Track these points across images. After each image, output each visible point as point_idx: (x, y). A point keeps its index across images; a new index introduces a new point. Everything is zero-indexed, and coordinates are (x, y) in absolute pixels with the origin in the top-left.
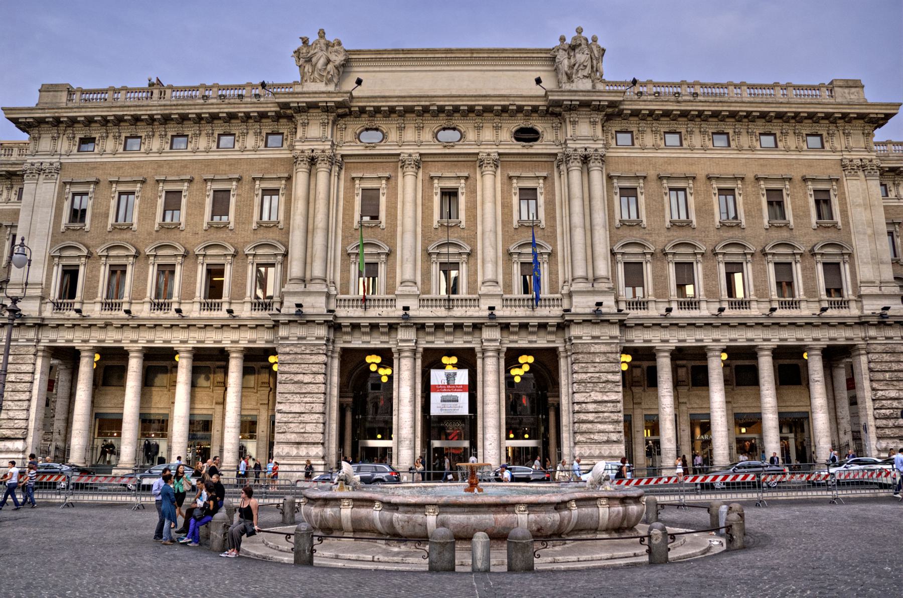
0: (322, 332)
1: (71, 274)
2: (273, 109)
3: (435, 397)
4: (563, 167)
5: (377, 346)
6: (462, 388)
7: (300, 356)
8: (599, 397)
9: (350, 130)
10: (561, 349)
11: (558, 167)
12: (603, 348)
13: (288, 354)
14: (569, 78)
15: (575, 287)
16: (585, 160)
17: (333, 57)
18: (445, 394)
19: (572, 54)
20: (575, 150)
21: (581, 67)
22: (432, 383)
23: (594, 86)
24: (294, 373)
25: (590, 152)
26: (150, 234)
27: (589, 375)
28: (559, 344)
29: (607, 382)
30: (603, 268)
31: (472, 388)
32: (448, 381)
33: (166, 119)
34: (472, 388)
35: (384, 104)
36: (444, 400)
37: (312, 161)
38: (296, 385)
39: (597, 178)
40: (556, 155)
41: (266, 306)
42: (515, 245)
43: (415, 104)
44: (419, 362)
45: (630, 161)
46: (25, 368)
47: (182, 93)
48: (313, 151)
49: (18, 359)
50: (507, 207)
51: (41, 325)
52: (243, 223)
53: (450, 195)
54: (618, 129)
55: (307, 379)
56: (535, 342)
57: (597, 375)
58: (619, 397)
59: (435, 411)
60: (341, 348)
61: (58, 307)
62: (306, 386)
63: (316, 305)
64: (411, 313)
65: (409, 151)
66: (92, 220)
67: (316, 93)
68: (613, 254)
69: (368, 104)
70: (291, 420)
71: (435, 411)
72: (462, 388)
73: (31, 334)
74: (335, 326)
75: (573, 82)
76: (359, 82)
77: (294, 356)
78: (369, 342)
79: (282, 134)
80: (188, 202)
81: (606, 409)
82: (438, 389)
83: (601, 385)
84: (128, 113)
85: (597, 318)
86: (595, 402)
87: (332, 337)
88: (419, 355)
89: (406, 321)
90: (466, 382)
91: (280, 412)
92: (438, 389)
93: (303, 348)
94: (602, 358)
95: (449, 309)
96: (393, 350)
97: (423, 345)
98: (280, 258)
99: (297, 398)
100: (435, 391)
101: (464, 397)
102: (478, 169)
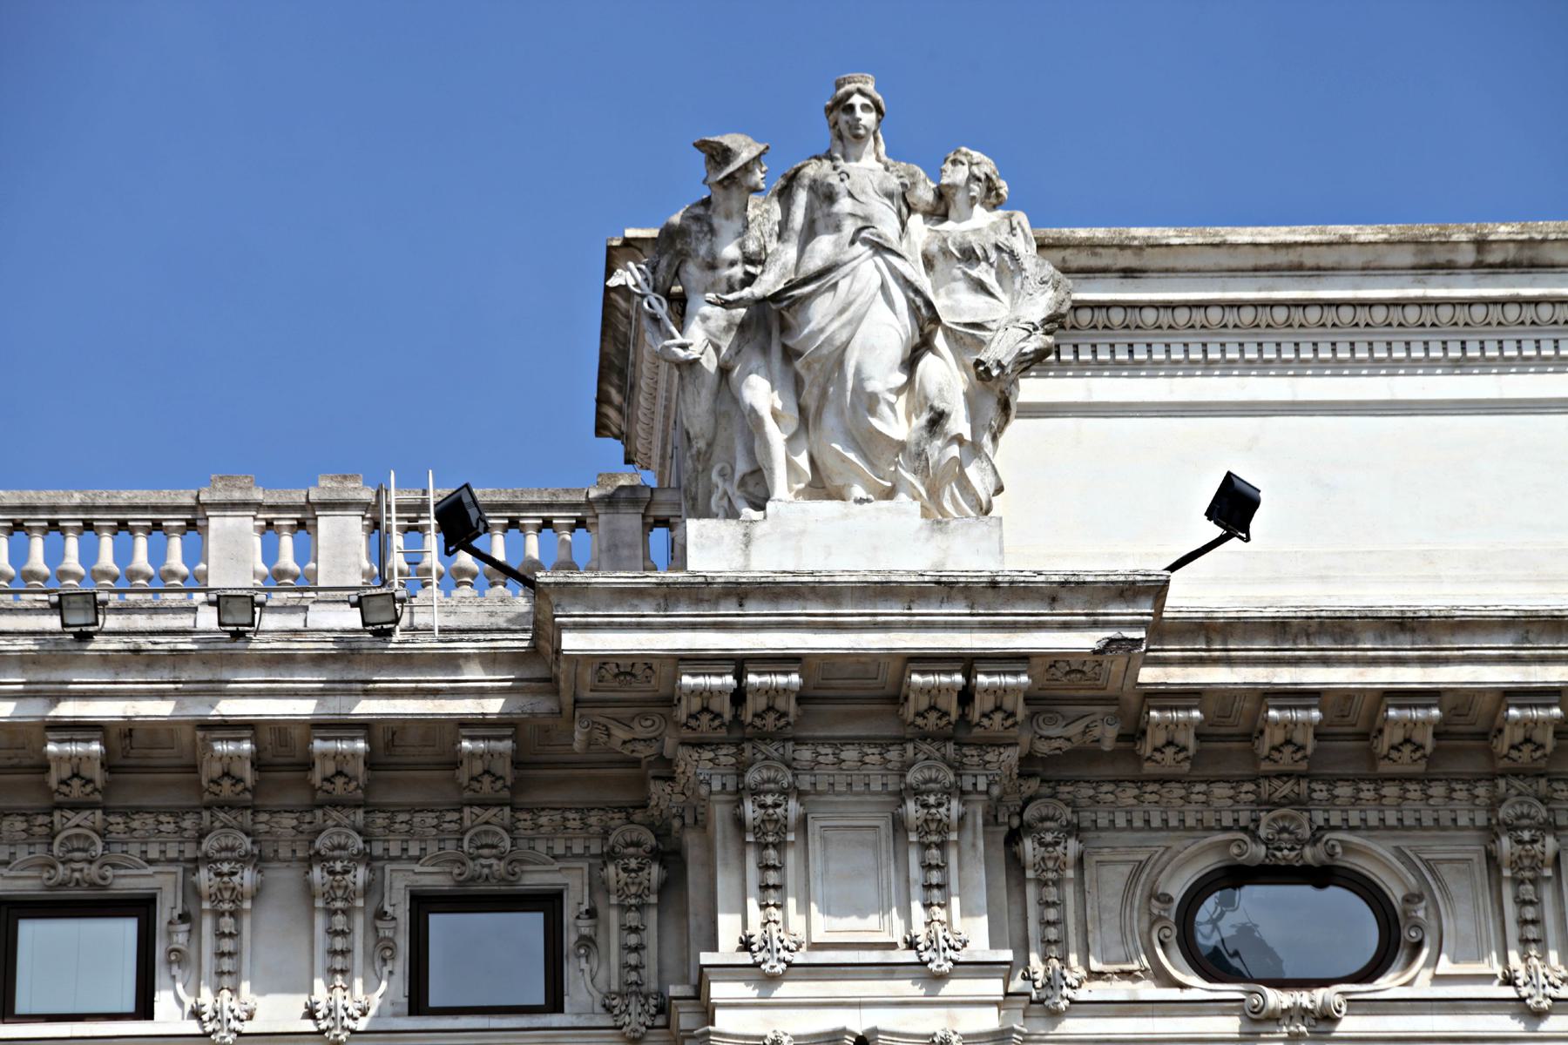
2: (494, 706)
9: (1111, 880)
17: (956, 304)
67: (884, 590)
69: (1284, 676)
76: (1234, 507)
79: (549, 903)
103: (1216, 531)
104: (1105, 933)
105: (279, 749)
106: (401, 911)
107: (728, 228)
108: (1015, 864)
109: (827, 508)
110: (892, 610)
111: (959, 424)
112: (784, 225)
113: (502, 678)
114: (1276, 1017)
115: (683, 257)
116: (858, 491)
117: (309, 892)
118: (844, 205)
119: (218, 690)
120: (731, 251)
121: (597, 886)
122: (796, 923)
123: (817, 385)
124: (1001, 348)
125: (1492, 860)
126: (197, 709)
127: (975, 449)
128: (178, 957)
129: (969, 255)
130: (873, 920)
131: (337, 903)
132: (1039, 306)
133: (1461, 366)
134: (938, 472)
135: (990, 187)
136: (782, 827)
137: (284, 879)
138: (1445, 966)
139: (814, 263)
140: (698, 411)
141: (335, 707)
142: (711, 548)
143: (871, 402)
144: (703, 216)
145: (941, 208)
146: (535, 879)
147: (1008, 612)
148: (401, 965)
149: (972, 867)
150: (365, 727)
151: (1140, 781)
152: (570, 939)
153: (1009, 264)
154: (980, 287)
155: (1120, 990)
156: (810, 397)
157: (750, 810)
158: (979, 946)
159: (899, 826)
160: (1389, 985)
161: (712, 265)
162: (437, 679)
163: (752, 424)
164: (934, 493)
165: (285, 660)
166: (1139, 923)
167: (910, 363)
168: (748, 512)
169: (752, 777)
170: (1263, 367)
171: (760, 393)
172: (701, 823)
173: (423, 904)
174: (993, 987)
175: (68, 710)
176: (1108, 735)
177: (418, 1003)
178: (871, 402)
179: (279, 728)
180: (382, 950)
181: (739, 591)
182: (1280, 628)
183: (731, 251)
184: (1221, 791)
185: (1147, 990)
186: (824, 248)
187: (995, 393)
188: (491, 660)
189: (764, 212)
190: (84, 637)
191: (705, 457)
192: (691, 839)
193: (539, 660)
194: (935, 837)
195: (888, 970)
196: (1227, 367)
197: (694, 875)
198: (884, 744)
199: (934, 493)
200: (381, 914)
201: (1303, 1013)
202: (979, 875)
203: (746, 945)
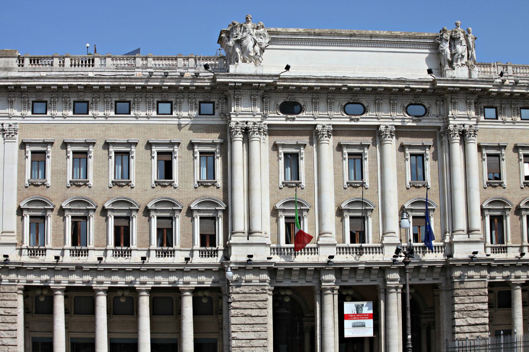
0: (265, 276)
1: (38, 222)
2: (209, 84)
3: (347, 323)
4: (445, 138)
5: (303, 285)
6: (369, 316)
7: (248, 295)
8: (472, 321)
10: (443, 285)
11: (441, 137)
12: (475, 285)
13: (238, 293)
14: (451, 64)
15: (456, 238)
16: (463, 134)
17: (259, 40)
18: (355, 321)
19: (453, 44)
20: (455, 126)
21: (460, 56)
23: (470, 73)
24: (244, 309)
25: (467, 127)
26: (104, 190)
27: (466, 305)
28: (441, 281)
29: (479, 310)
30: (477, 223)
31: (376, 317)
33: (114, 89)
35: (305, 84)
37: (246, 132)
38: (247, 318)
39: (473, 148)
40: (439, 128)
41: (214, 253)
42: (409, 203)
43: (330, 84)
44: (336, 297)
45: (495, 132)
46: (10, 304)
47: (119, 62)
48: (247, 122)
49: (3, 296)
50: (400, 170)
51: (21, 269)
52: (186, 182)
53: (356, 158)
54: (486, 105)
55: (254, 313)
57: (471, 305)
58: (487, 321)
61: (33, 252)
62: (254, 318)
63: (261, 255)
64: (334, 260)
65: (324, 123)
66: (51, 176)
67: (251, 75)
68: (482, 210)
69: (292, 84)
70: (244, 345)
71: (349, 333)
72: (369, 316)
73: (13, 276)
74: (273, 271)
75: (454, 69)
76: (288, 68)
77: (243, 295)
80: (137, 162)
81: (477, 330)
82: (349, 317)
83: (474, 312)
84: (82, 83)
85: (473, 263)
86: (470, 325)
89: (329, 266)
90: (371, 312)
91: (234, 339)
92: (349, 317)
93: (250, 288)
94: (476, 292)
95: (361, 255)
98: (220, 214)
99: (247, 328)
100: (347, 319)
101: (370, 323)
102: (377, 138)
103: (285, 70)
104: (272, 108)
105: (186, 87)
106: (198, 103)
107: (234, 31)
108: (263, 101)
109: (245, 64)
110: (251, 77)
111: (259, 54)
112: (241, 30)
113: (210, 81)
114: (289, 118)
115: (229, 34)
116: (248, 62)
117: (188, 101)
118: (247, 29)
119: (180, 82)
120: (235, 34)
121: (219, 101)
122: (240, 108)
123: (244, 50)
124: (263, 46)
125: (312, 102)
126: (178, 84)
127: (260, 56)
128: (175, 108)
129: (260, 35)
130: (248, 108)
131: (191, 103)
132: (267, 41)
133: (312, 45)
134: (256, 59)
135: (263, 26)
136: (239, 98)
137: (186, 100)
138: (307, 113)
139: (244, 36)
140: (231, 51)
141: (192, 84)
142: (232, 69)
143: (250, 52)
144: (232, 30)
145: (257, 28)
146: (212, 100)
147: (264, 78)
148: (198, 109)
149: (259, 102)
150: (195, 86)
151: (276, 92)
152: (216, 107)
153: (264, 36)
154: (261, 38)
155: (273, 115)
156: (243, 50)
157: (236, 97)
158: (259, 112)
159: (251, 98)
160: (300, 115)
161: (233, 35)
162: (203, 81)
163: (237, 54)
164: (256, 61)
165: (187, 79)
166: (275, 107)
167: (254, 47)
168: (236, 63)
169: (236, 93)
170: (291, 45)
171: (238, 50)
172: (230, 96)
173: (200, 102)
174: (260, 116)
175: (165, 84)
176: (273, 89)
177: (200, 114)
178: (250, 52)
179: (186, 86)
180: (196, 108)
181: (236, 75)
182: (292, 79)
183: (235, 34)
184: (285, 94)
185: (276, 115)
186: (245, 34)
187: (262, 50)
188: (208, 79)
189: (238, 29)
190: (166, 76)
191: (231, 55)
192: (229, 98)
193: (214, 79)
194: (255, 100)
195: (249, 114)
196: (287, 45)
197: (229, 102)
198: (250, 90)
199: (256, 61)
200: (196, 104)
201: (292, 118)
202: (259, 104)
203: (235, 111)
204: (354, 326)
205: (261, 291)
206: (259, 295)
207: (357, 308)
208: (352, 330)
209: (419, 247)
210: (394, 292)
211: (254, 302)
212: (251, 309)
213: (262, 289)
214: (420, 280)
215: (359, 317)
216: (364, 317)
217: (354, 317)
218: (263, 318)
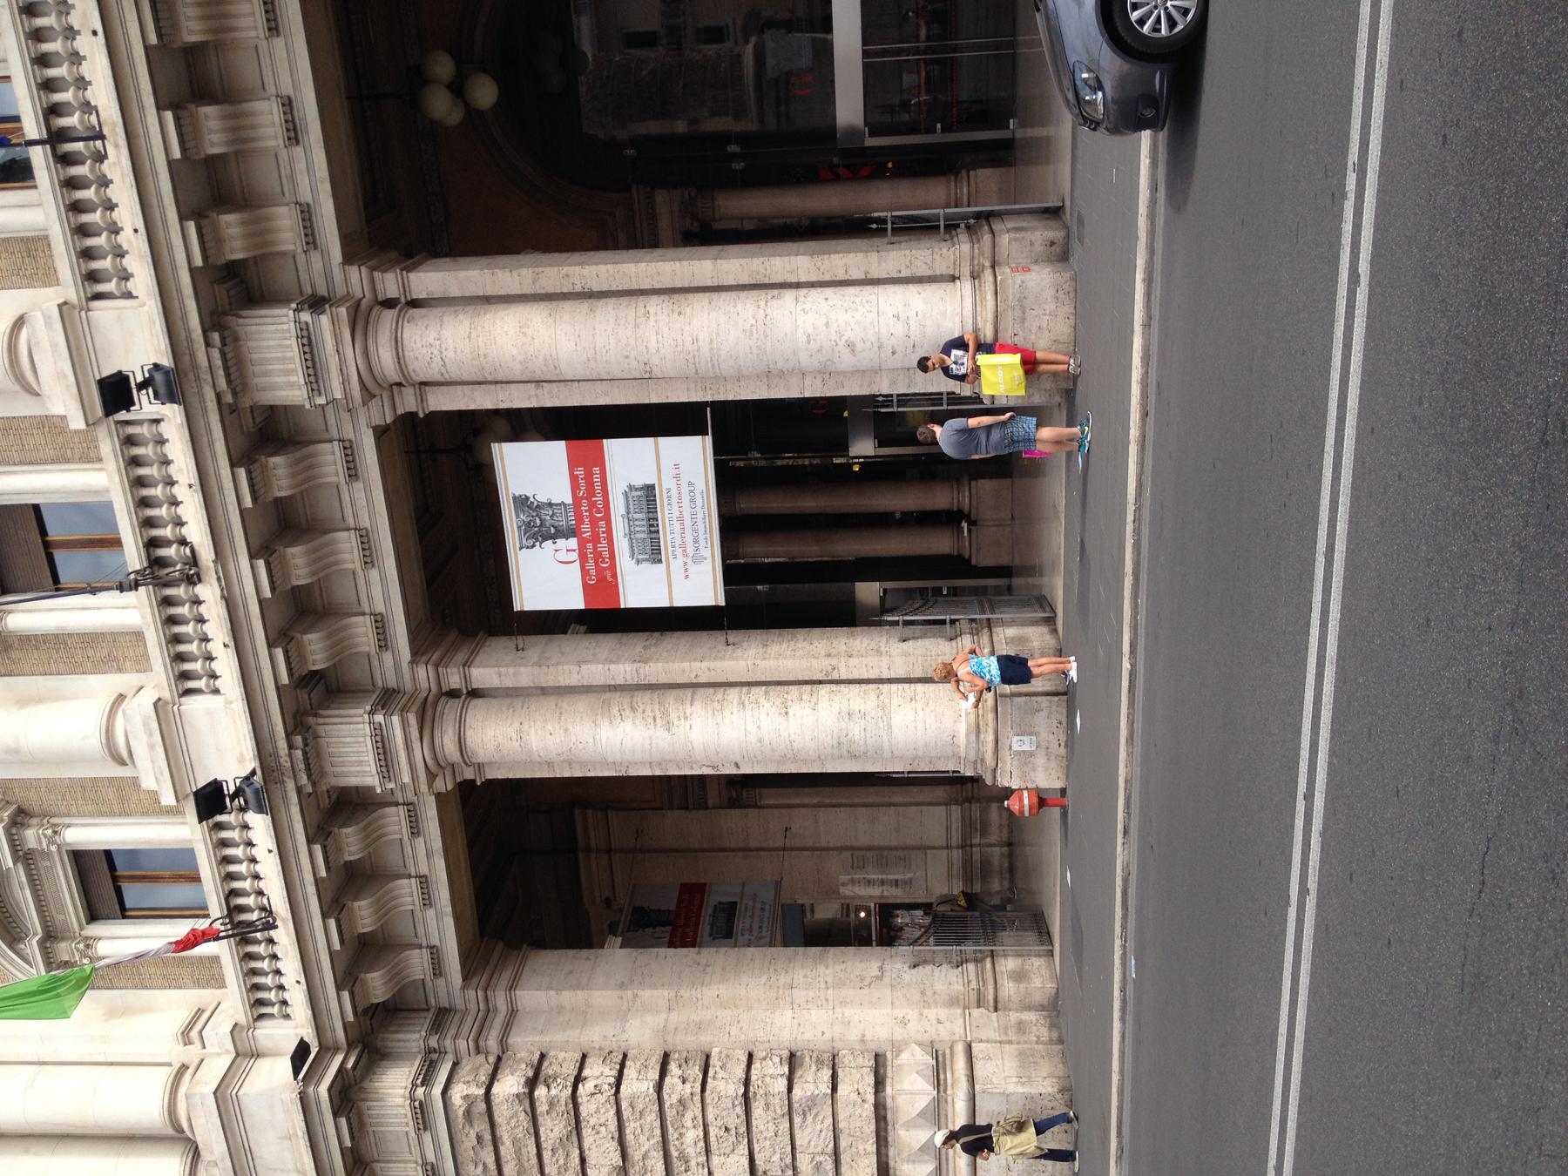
3: (641, 588)
5: (437, 844)
22: (581, 605)
32: (560, 534)
34: (584, 426)
36: (655, 555)
56: (288, 104)
59: (701, 585)
60: (467, 975)
62: (635, 1155)
71: (701, 585)
78: (424, 881)
82: (601, 579)
87: (413, 1038)
88: (454, 679)
90: (557, 451)
96: (444, 784)
97: (397, 662)
101: (629, 460)
204: (655, 555)
205: (482, 1126)
206: (504, 1134)
207: (541, 531)
208: (676, 565)
209: (65, 160)
210: (397, 343)
211: (546, 1155)
212: (583, 1160)
213: (468, 1113)
214: (294, 135)
215: (594, 523)
216: (591, 492)
217: (598, 556)
218: (626, 1114)
